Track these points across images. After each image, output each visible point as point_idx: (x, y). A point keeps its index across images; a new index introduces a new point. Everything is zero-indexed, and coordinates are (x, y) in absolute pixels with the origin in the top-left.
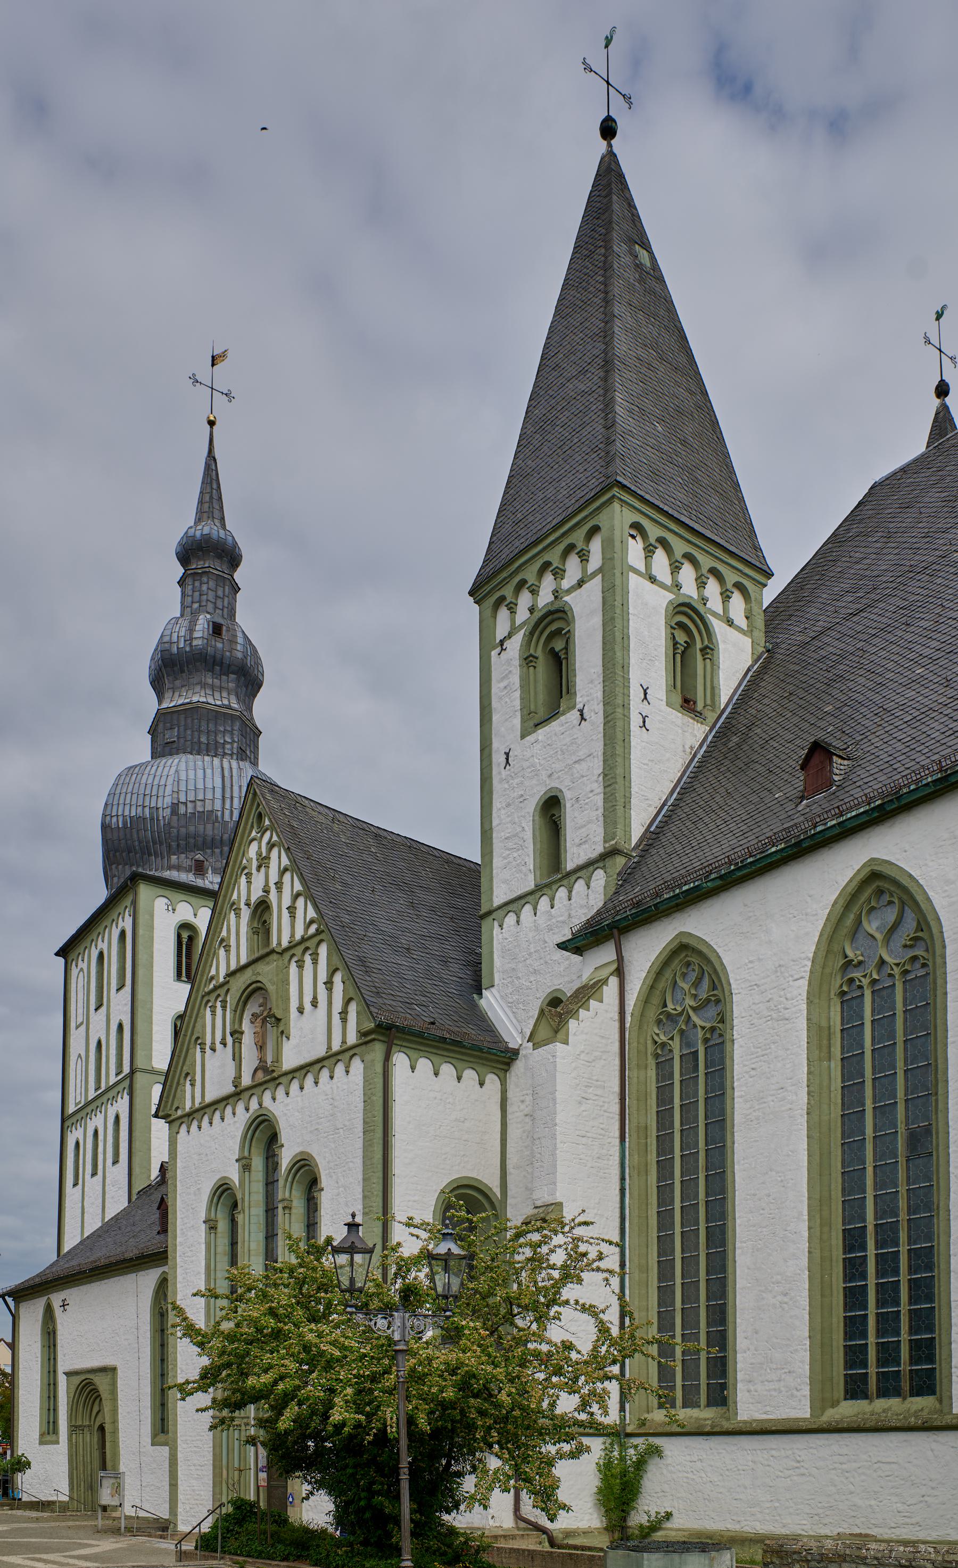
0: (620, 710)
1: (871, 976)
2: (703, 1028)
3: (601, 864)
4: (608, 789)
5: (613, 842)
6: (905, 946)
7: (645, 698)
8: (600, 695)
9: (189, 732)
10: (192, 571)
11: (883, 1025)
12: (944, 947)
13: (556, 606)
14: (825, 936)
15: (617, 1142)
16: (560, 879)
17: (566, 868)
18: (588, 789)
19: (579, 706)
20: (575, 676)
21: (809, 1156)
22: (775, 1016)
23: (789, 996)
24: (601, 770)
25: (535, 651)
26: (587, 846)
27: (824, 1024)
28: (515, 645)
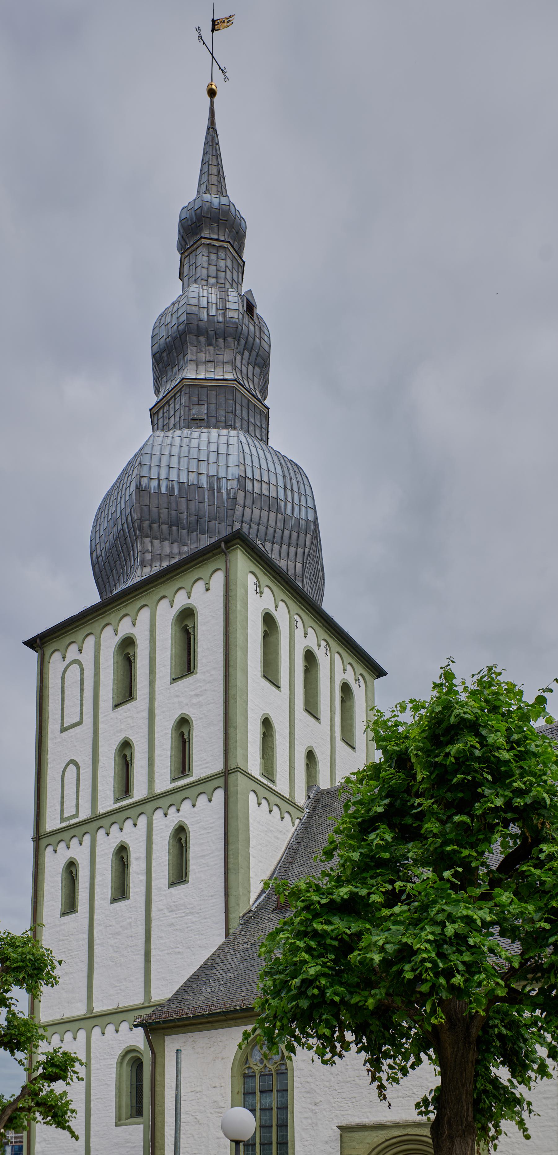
9: (222, 413)
10: (208, 241)
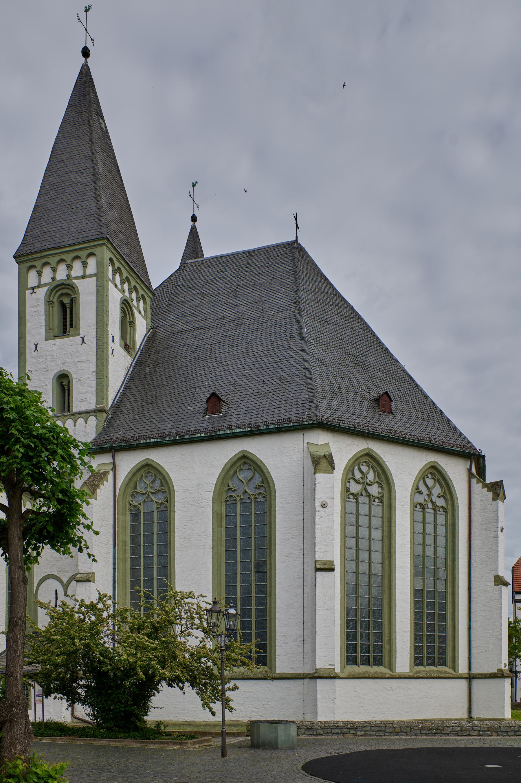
0: (105, 345)
1: (241, 497)
2: (157, 503)
3: (94, 414)
4: (99, 380)
5: (102, 406)
6: (256, 488)
7: (113, 341)
8: (94, 334)
11: (246, 518)
12: (275, 492)
13: (68, 282)
14: (222, 476)
15: (112, 546)
16: (69, 415)
17: (72, 410)
18: (87, 376)
19: (83, 336)
20: (79, 320)
21: (213, 566)
22: (196, 505)
23: (203, 497)
24: (94, 369)
25: (53, 299)
26: (85, 403)
27: (219, 512)
28: (42, 292)
